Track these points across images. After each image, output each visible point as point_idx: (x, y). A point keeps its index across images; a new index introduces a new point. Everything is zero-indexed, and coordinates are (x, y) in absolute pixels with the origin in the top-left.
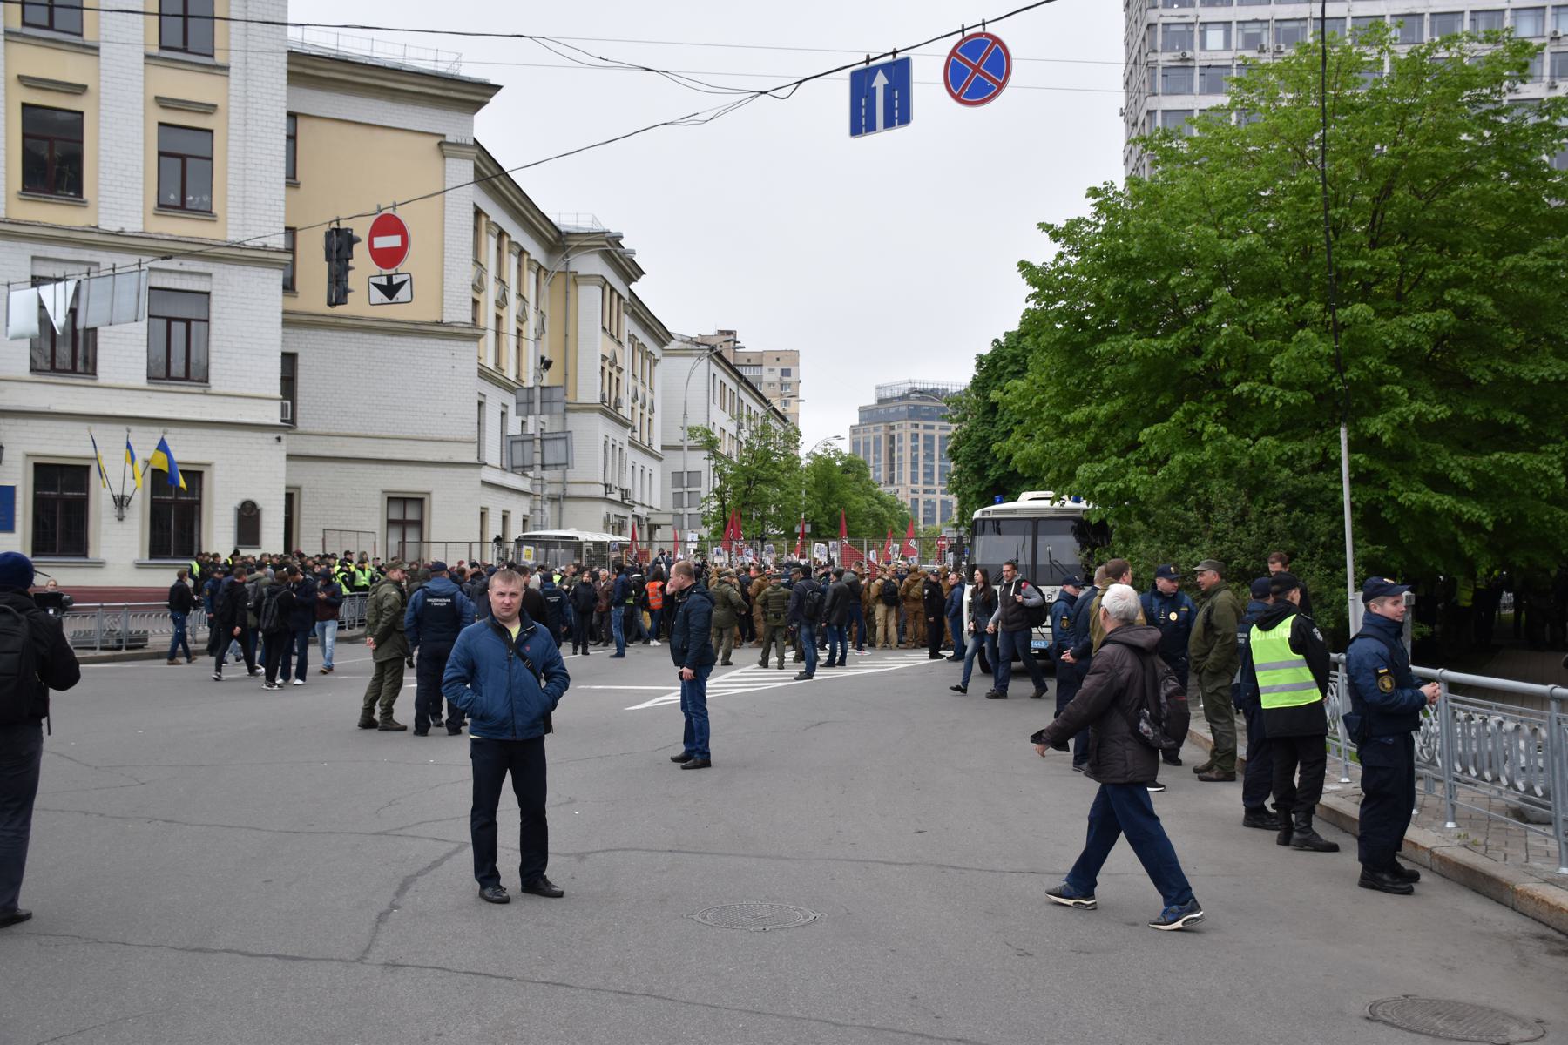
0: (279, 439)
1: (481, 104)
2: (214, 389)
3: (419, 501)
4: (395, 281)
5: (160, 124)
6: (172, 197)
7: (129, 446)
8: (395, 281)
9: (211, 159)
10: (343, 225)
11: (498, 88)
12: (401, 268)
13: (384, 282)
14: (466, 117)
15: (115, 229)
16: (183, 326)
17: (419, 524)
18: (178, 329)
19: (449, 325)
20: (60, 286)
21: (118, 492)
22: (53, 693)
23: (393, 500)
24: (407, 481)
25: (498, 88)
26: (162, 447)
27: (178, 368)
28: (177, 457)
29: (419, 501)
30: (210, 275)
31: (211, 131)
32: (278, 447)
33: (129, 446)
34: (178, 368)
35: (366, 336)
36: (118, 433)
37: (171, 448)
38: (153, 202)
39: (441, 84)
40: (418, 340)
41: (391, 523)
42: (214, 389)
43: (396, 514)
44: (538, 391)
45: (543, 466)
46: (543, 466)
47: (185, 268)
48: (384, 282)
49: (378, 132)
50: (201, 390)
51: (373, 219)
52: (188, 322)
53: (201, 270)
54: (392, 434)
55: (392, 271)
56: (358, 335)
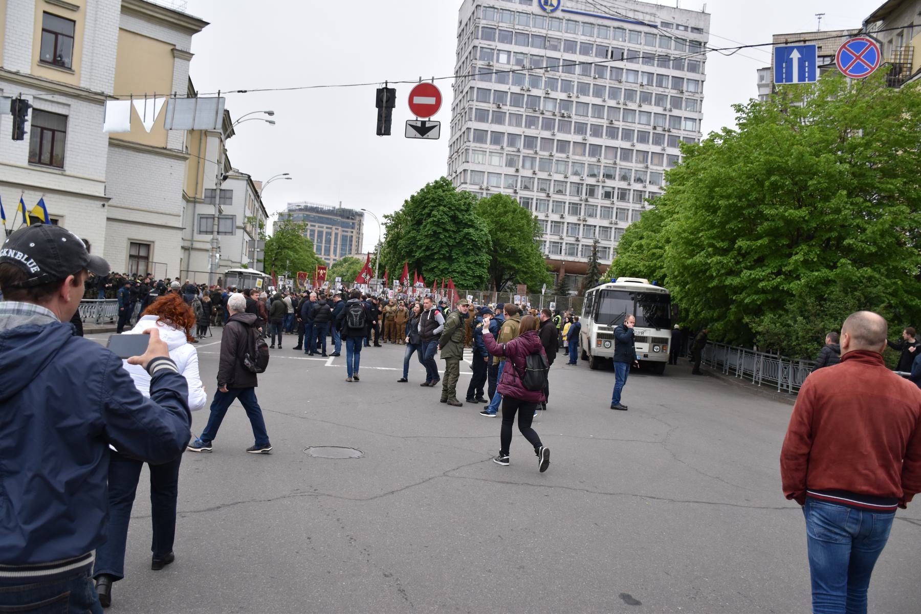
0: (104, 205)
1: (197, 31)
2: (67, 173)
3: (147, 246)
4: (427, 125)
5: (44, 12)
6: (48, 56)
7: (22, 201)
8: (427, 125)
9: (73, 38)
10: (390, 86)
11: (208, 24)
12: (433, 118)
13: (419, 124)
14: (188, 37)
15: (14, 70)
16: (50, 133)
17: (146, 258)
18: (48, 135)
19: (170, 150)
20: (150, 101)
21: (9, 228)
22: (258, 375)
23: (135, 244)
24: (143, 234)
25: (208, 24)
26: (41, 204)
27: (46, 157)
28: (49, 211)
29: (147, 246)
30: (69, 105)
31: (74, 22)
32: (102, 210)
33: (22, 201)
34: (46, 157)
35: (125, 151)
36: (17, 194)
37: (46, 206)
38: (38, 58)
39: (177, 17)
40: (153, 156)
41: (131, 256)
42: (67, 173)
43: (134, 253)
44: (218, 191)
45: (218, 233)
46: (218, 233)
47: (55, 99)
48: (419, 124)
49: (139, 38)
50: (60, 172)
51: (413, 86)
52: (53, 131)
53: (64, 102)
54: (135, 207)
55: (427, 119)
56: (120, 150)
